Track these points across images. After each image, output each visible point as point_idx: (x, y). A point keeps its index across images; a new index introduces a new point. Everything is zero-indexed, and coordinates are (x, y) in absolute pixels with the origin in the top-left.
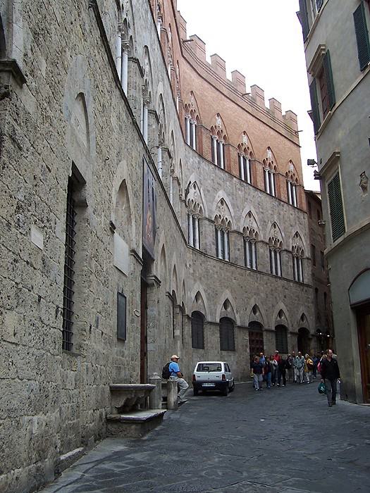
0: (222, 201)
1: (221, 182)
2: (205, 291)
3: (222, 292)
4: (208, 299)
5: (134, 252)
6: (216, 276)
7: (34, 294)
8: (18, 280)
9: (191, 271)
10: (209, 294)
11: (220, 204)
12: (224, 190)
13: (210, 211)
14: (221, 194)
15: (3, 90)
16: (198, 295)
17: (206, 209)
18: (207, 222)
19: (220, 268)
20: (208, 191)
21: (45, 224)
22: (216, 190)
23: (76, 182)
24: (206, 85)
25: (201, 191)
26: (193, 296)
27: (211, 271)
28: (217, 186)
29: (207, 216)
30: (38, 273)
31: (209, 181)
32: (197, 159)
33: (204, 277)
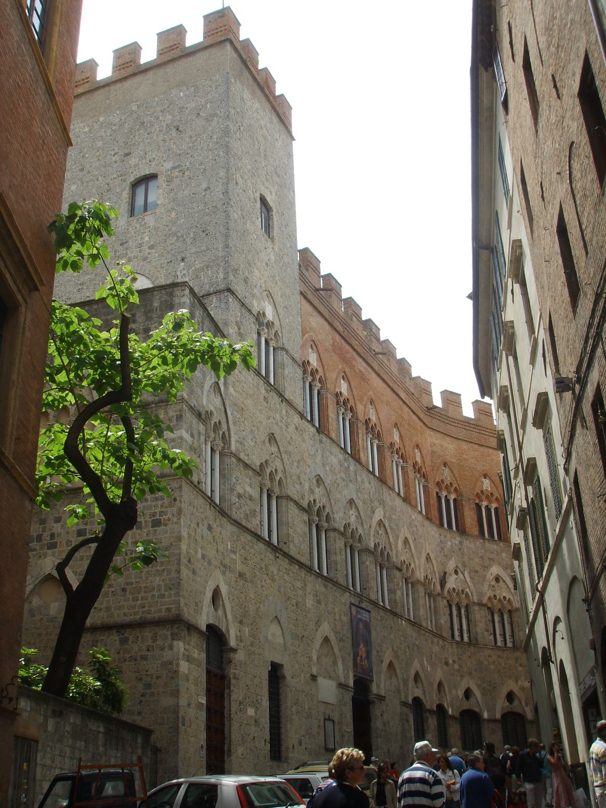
0: (497, 579)
1: (492, 556)
2: (479, 686)
3: (503, 684)
4: (483, 694)
5: (342, 686)
6: (492, 667)
7: (251, 737)
8: (243, 733)
9: (456, 666)
10: (484, 689)
11: (493, 583)
12: (499, 564)
13: (481, 594)
14: (495, 570)
15: (229, 660)
16: (468, 693)
17: (474, 594)
18: (476, 608)
19: (499, 657)
20: (476, 572)
21: (256, 705)
22: (486, 568)
23: (276, 673)
24: (465, 446)
25: (466, 574)
26: (461, 693)
27: (486, 662)
28: (487, 562)
29: (476, 601)
30: (253, 727)
31: (477, 560)
32: (458, 539)
33: (476, 670)
